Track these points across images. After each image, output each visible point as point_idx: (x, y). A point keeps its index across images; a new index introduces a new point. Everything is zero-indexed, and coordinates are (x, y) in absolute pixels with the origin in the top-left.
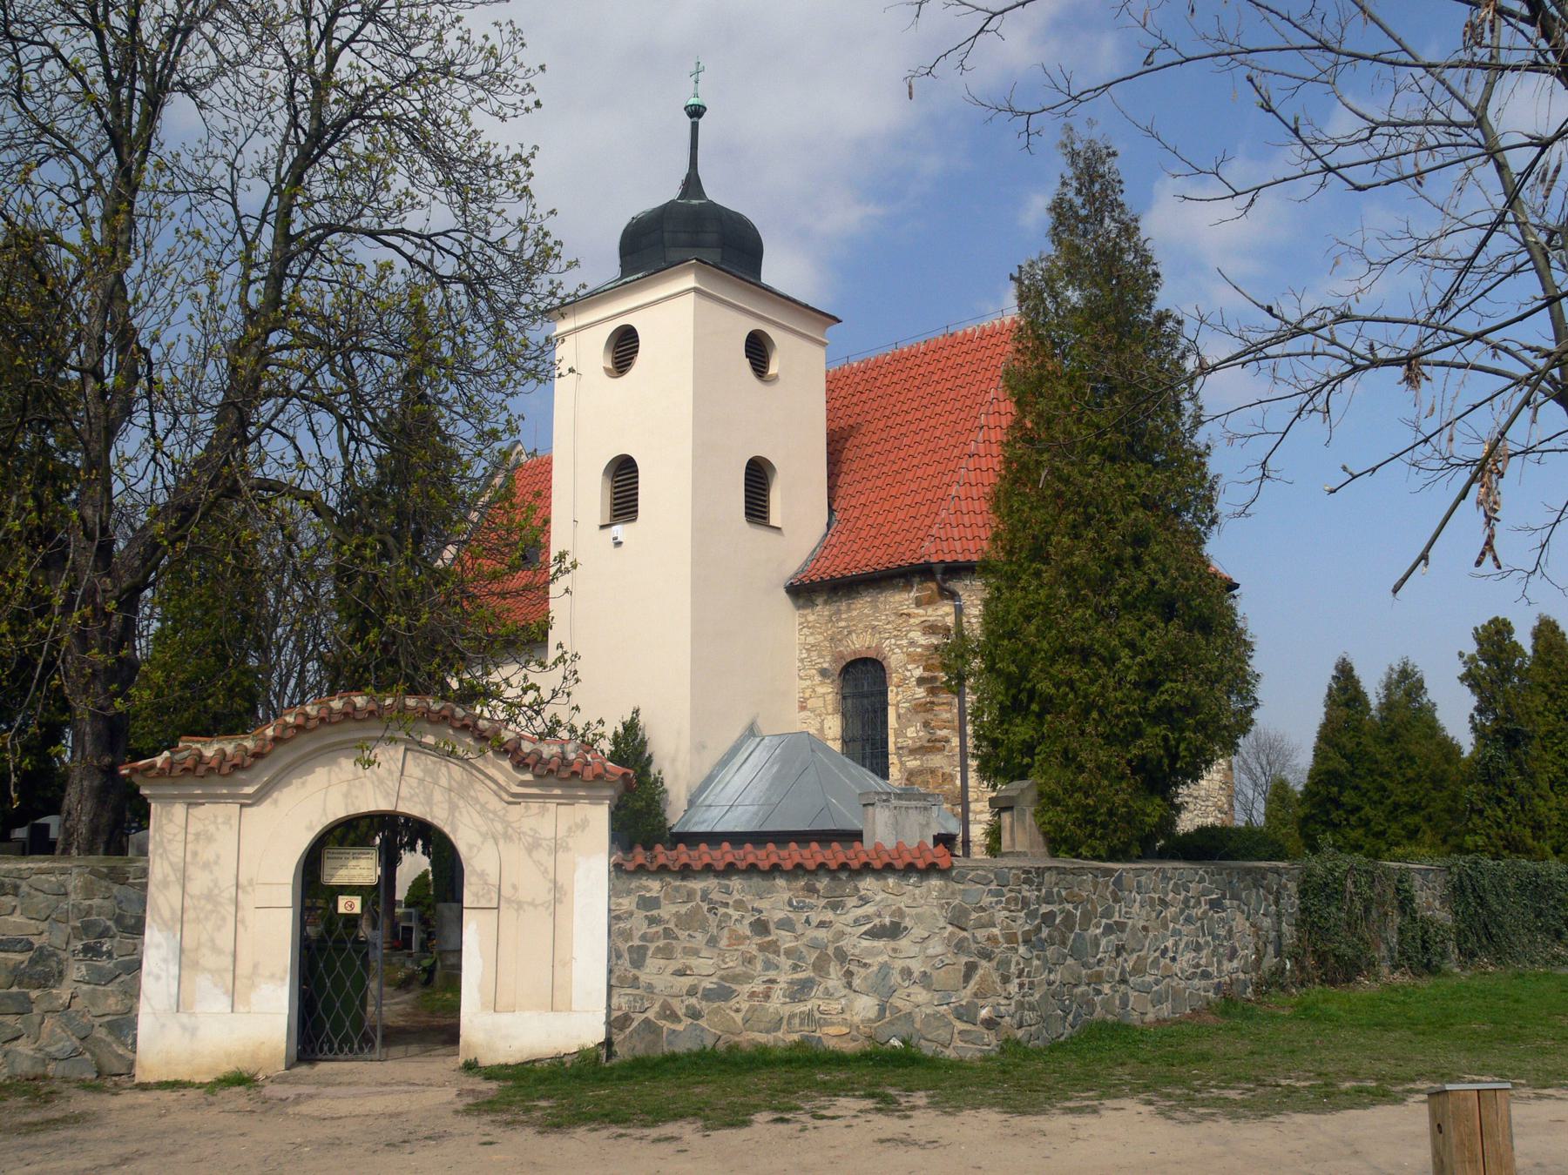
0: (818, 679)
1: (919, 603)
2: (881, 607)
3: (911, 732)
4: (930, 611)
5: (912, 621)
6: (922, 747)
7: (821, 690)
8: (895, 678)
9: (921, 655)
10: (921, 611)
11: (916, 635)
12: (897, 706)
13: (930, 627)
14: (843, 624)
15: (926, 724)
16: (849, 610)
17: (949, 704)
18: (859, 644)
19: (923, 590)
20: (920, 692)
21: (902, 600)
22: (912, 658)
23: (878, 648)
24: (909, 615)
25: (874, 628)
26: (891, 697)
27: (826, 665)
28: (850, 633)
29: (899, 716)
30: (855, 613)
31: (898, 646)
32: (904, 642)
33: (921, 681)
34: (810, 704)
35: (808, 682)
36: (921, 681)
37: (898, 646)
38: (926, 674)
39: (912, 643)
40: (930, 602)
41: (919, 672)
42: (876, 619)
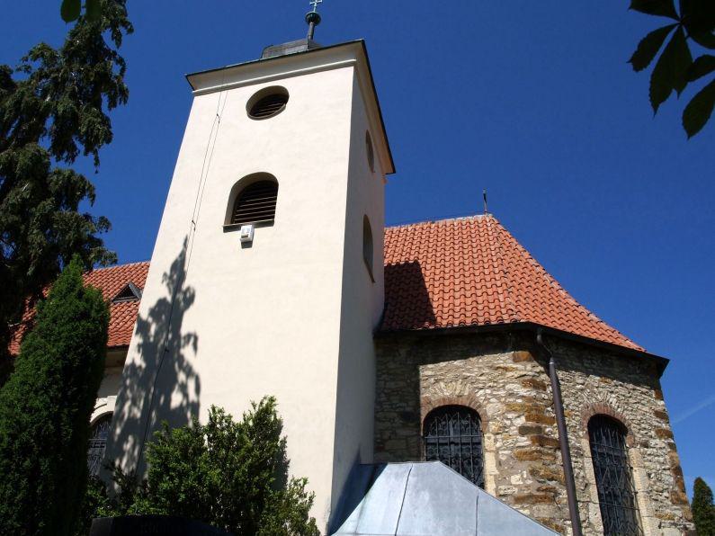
0: (399, 421)
3: (515, 479)
5: (509, 374)
6: (531, 496)
7: (403, 432)
8: (493, 426)
9: (522, 406)
14: (430, 373)
15: (533, 473)
20: (524, 441)
24: (506, 369)
26: (488, 442)
27: (408, 409)
29: (499, 464)
31: (495, 396)
32: (502, 393)
33: (523, 431)
34: (388, 445)
35: (388, 424)
36: (523, 431)
37: (495, 396)
38: (530, 424)
41: (521, 421)
42: (468, 370)
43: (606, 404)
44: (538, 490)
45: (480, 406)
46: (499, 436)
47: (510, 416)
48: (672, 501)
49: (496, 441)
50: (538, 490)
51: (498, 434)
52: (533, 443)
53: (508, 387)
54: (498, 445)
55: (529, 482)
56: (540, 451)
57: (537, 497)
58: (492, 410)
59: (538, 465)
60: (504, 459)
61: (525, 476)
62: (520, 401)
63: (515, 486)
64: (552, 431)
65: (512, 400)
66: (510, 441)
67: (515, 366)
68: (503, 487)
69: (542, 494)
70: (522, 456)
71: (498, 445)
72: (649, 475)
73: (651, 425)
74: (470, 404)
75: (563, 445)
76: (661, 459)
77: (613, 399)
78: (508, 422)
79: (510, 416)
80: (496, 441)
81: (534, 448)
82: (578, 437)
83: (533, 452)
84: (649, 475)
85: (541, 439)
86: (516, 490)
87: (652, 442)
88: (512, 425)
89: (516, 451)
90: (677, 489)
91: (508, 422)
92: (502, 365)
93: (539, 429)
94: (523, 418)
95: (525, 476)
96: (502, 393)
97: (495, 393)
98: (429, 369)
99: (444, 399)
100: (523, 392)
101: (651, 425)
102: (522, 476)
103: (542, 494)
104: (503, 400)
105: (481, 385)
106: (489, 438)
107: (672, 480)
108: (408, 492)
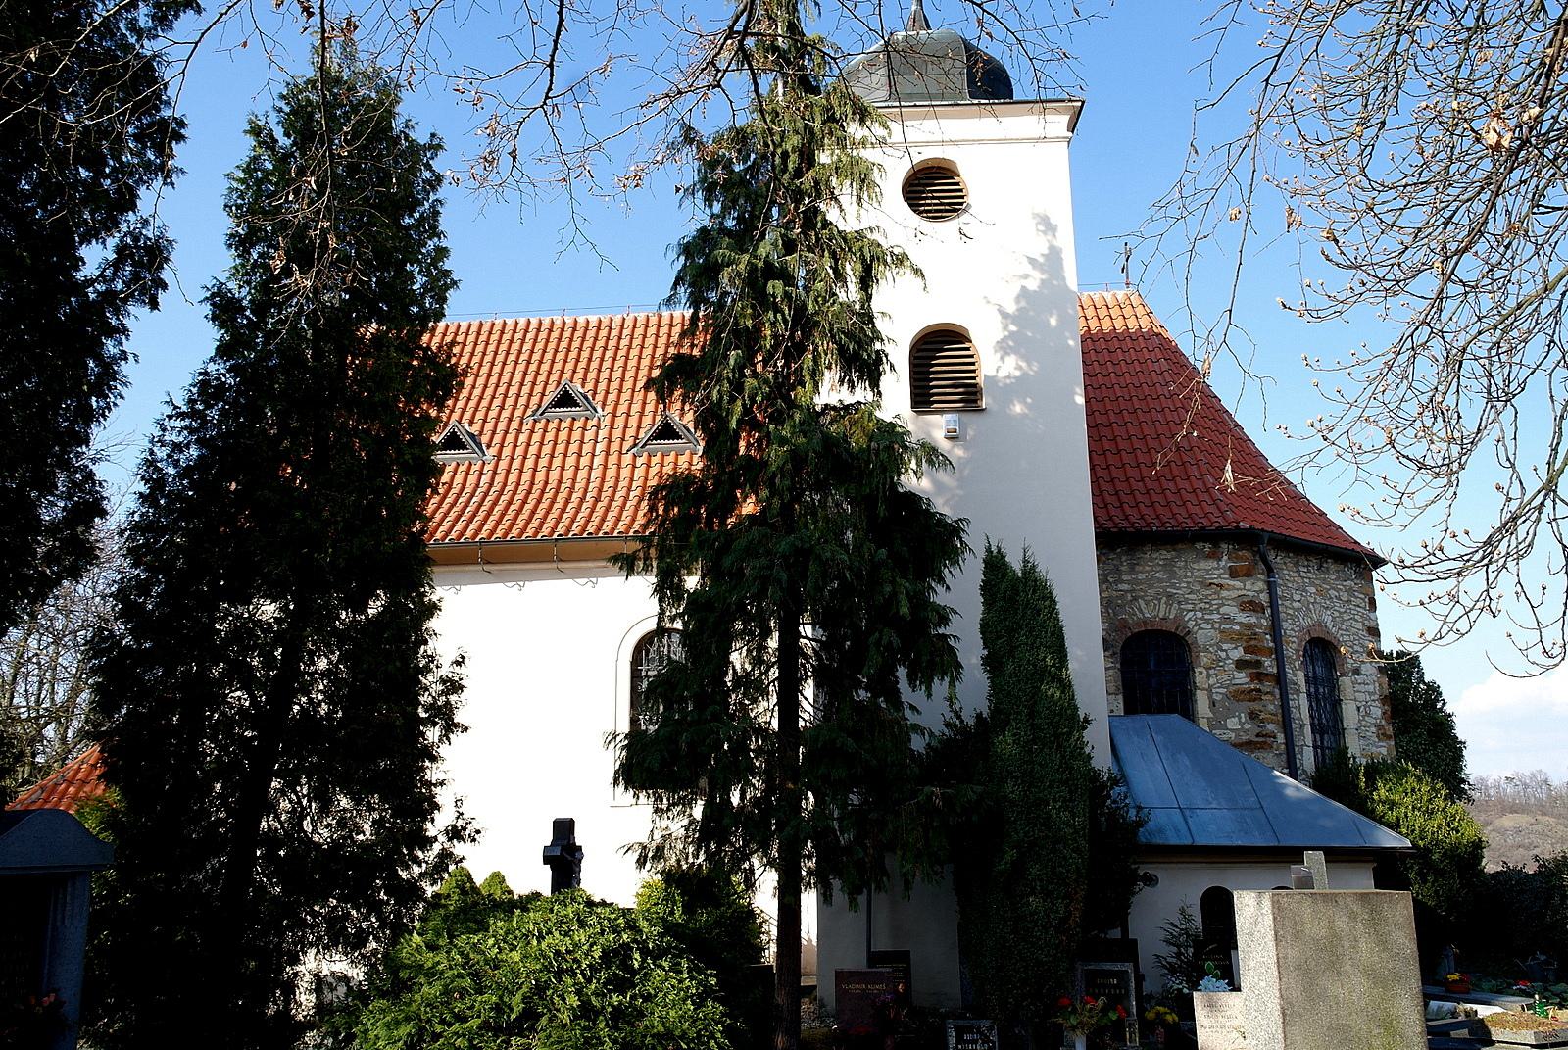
1: (1233, 574)
2: (1181, 572)
3: (1232, 723)
4: (1248, 585)
5: (1224, 594)
8: (1205, 659)
10: (1237, 584)
11: (1231, 610)
12: (1210, 690)
13: (1251, 603)
14: (1126, 587)
15: (1253, 716)
16: (1132, 570)
17: (1271, 693)
18: (1151, 611)
19: (1238, 558)
20: (1242, 678)
21: (1215, 568)
22: (1228, 636)
23: (1179, 618)
24: (1221, 586)
25: (1170, 596)
26: (1200, 677)
28: (1135, 599)
29: (1213, 704)
30: (1141, 576)
31: (1207, 621)
32: (1216, 617)
33: (1241, 664)
36: (1241, 664)
38: (1248, 657)
39: (1227, 619)
40: (1248, 574)
41: (1238, 653)
42: (1173, 586)
43: (1320, 624)
44: (1258, 736)
45: (1189, 632)
46: (1212, 671)
47: (1225, 647)
48: (1378, 737)
49: (1209, 676)
50: (1258, 736)
51: (1211, 668)
52: (1252, 681)
53: (1222, 610)
54: (1212, 681)
55: (1247, 726)
56: (1259, 691)
57: (1258, 742)
58: (1204, 635)
59: (1256, 706)
60: (1218, 698)
61: (1243, 720)
62: (1237, 628)
63: (1231, 730)
64: (1269, 665)
65: (1227, 626)
66: (1226, 677)
67: (1231, 583)
68: (1218, 732)
69: (1261, 740)
70: (1238, 695)
71: (1212, 681)
72: (1359, 708)
73: (1363, 646)
74: (1177, 629)
75: (1280, 679)
76: (1371, 688)
77: (1327, 619)
78: (1223, 655)
79: (1225, 647)
80: (1209, 676)
81: (1253, 687)
82: (1294, 669)
83: (1253, 690)
84: (1359, 708)
85: (1259, 677)
86: (1233, 735)
87: (1364, 669)
88: (1228, 658)
89: (1232, 689)
90: (1383, 722)
91: (1223, 655)
92: (1215, 581)
93: (1259, 664)
94: (1241, 649)
95: (1243, 720)
96: (1216, 617)
97: (1206, 617)
98: (1123, 582)
99: (1145, 623)
100: (1243, 618)
101: (1363, 646)
102: (1240, 718)
103: (1261, 740)
104: (1217, 626)
105: (1190, 607)
106: (1201, 673)
107: (1379, 712)
108: (1163, 755)
